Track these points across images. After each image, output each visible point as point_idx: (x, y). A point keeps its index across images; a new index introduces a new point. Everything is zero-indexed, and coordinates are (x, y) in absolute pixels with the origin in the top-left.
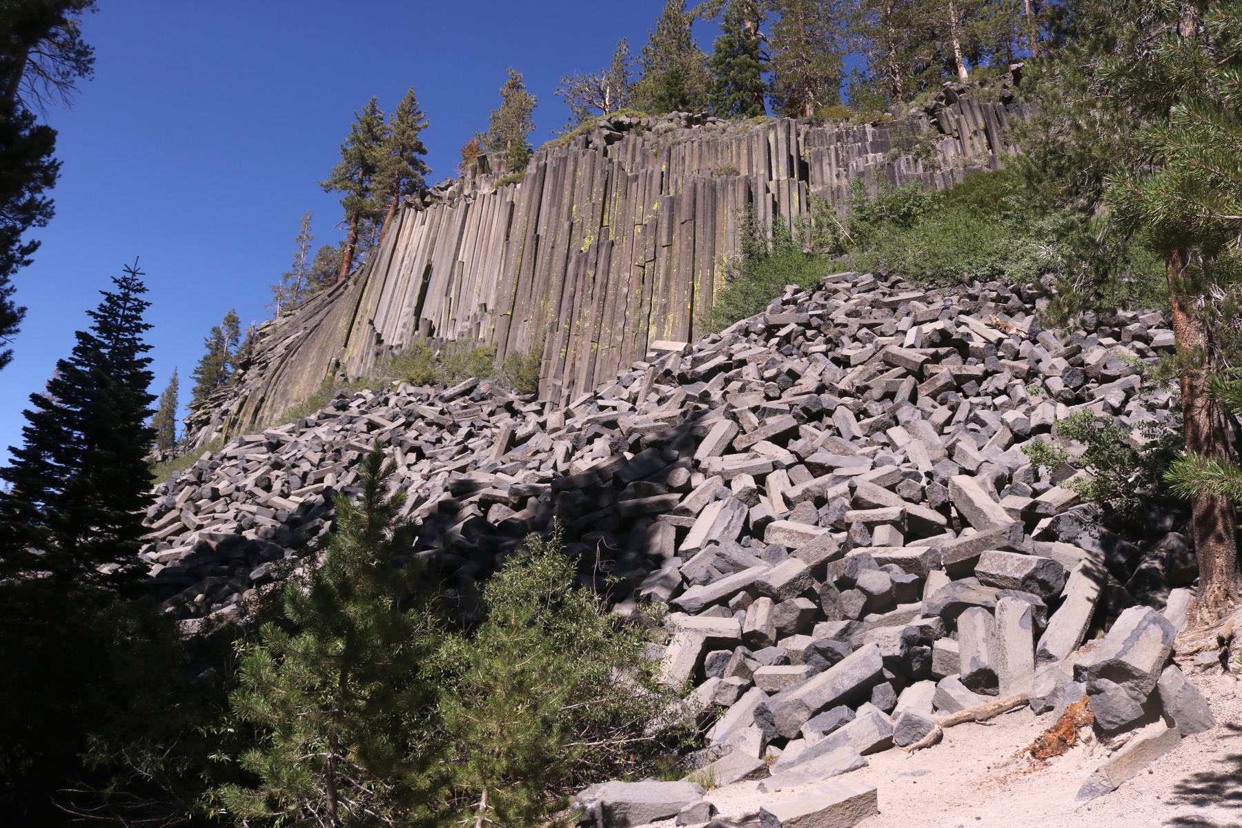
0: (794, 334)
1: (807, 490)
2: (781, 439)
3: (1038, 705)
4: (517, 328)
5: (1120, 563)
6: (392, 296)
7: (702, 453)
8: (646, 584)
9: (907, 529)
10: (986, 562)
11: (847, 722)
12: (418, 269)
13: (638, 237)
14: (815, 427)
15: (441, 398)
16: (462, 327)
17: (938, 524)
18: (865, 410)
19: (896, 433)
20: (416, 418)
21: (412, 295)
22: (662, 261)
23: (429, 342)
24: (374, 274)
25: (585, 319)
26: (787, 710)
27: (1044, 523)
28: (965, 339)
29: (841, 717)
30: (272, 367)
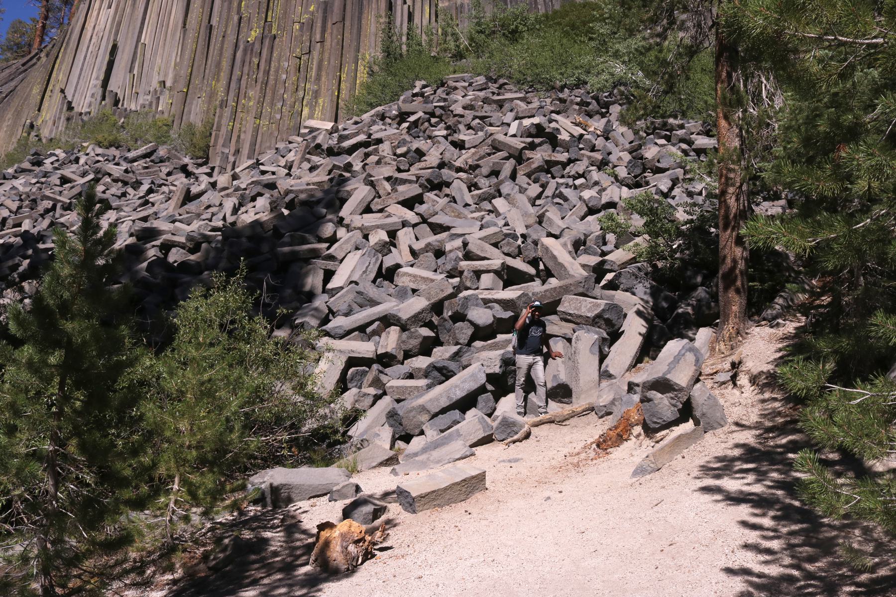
0: (421, 120)
1: (429, 244)
2: (409, 203)
3: (600, 411)
4: (191, 103)
5: (663, 308)
6: (81, 70)
7: (345, 212)
8: (300, 314)
9: (505, 277)
10: (566, 304)
11: (459, 422)
13: (296, 33)
14: (436, 195)
15: (126, 159)
16: (144, 100)
17: (529, 274)
18: (476, 183)
19: (499, 203)
20: (104, 175)
21: (99, 69)
22: (315, 54)
24: (65, 49)
25: (250, 99)
26: (412, 414)
27: (609, 276)
28: (555, 132)
29: (454, 418)
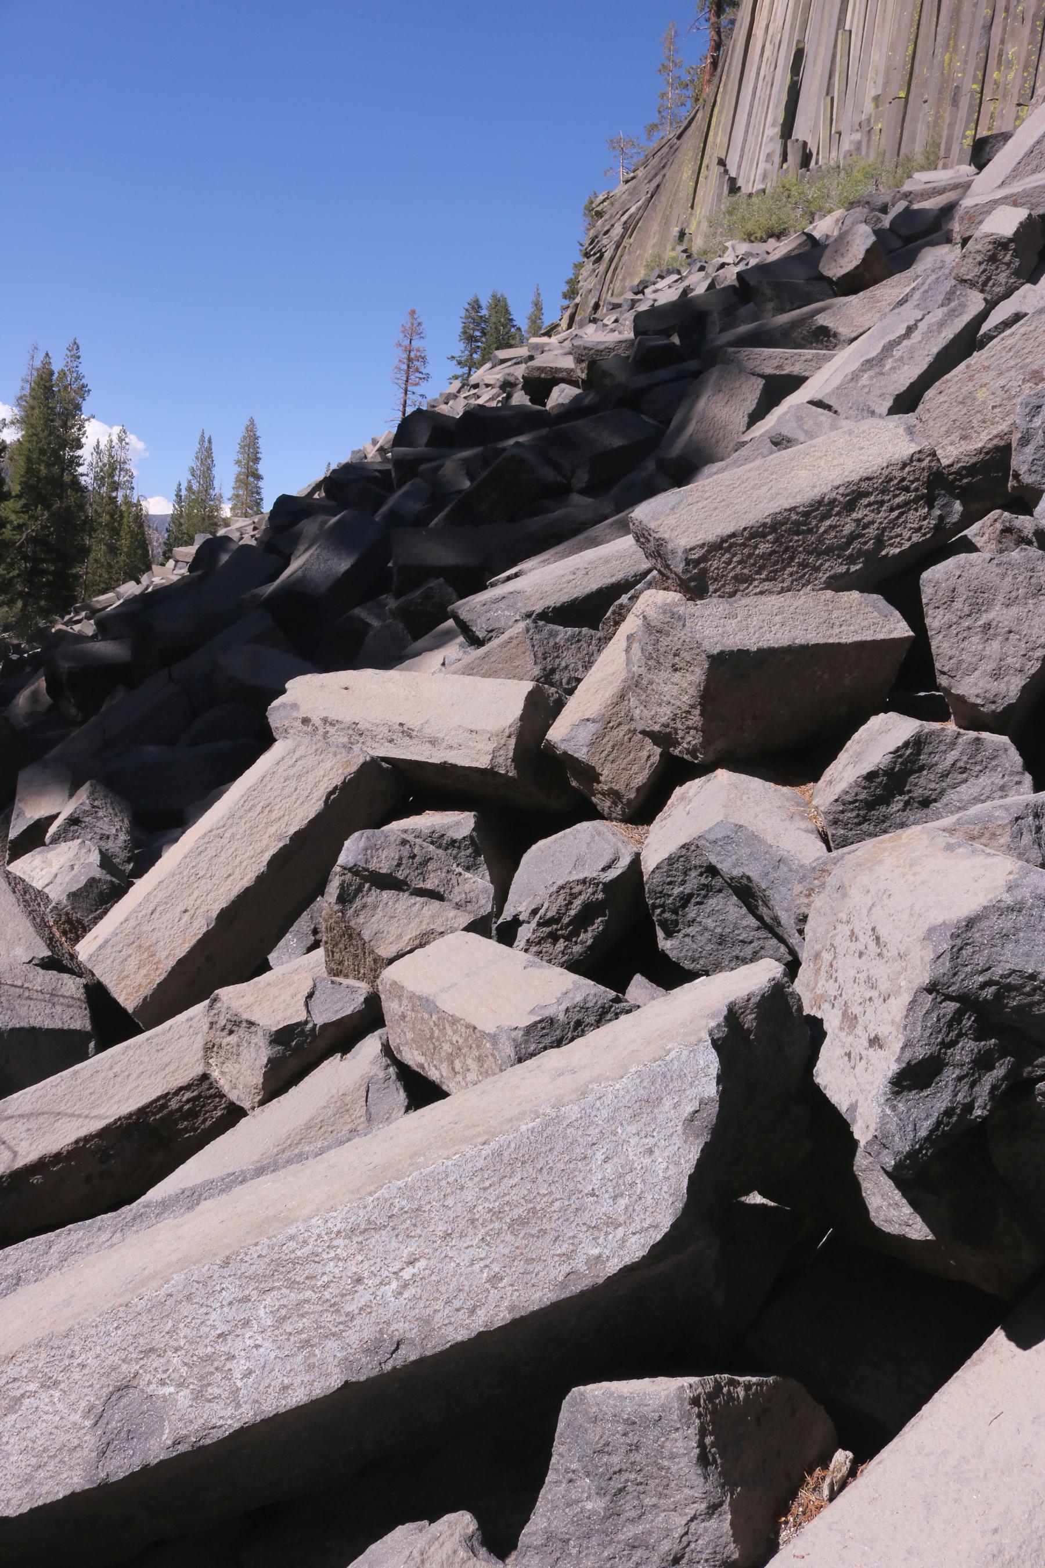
12: (785, 59)
16: (851, 142)
23: (803, 176)
30: (607, 255)
